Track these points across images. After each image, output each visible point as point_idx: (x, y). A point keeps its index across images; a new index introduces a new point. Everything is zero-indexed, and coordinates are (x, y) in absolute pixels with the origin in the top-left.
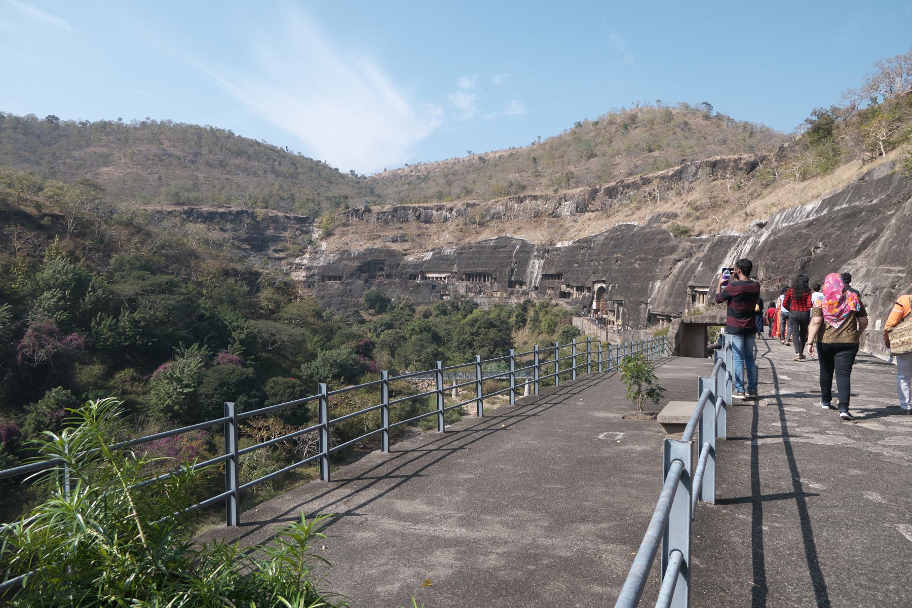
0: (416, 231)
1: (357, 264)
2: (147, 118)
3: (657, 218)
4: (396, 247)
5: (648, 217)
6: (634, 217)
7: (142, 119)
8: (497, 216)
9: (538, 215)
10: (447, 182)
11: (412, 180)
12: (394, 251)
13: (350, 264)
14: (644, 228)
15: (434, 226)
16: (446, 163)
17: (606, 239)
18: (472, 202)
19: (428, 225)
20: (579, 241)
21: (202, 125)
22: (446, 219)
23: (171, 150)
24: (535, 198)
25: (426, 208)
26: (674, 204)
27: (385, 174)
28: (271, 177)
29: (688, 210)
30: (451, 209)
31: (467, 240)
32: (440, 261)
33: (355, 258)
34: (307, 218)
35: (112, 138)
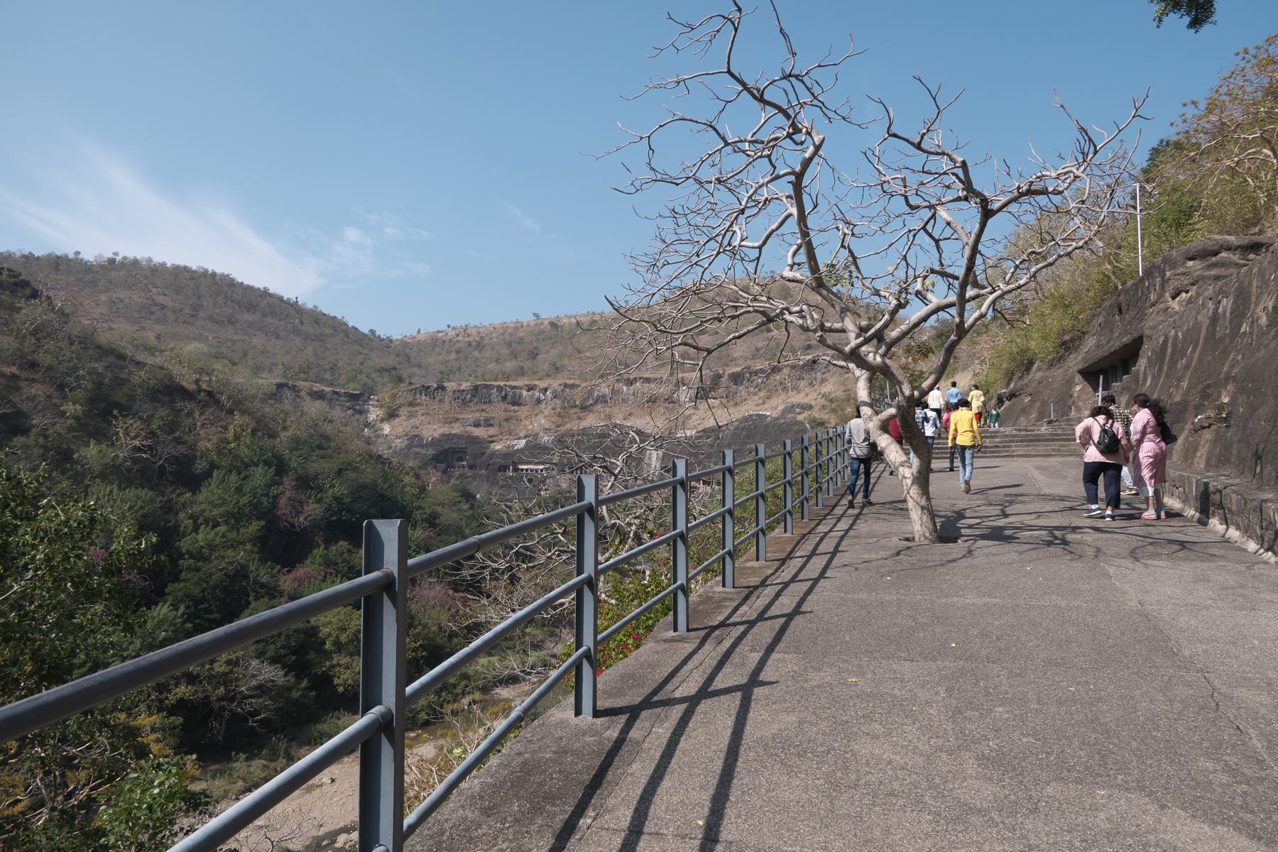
0: (503, 415)
1: (431, 452)
2: (116, 254)
3: (791, 409)
4: (479, 432)
5: (781, 408)
6: (766, 406)
7: (108, 255)
8: (602, 400)
9: (653, 400)
10: (512, 352)
11: (465, 348)
12: (477, 437)
13: (423, 451)
14: (777, 418)
15: (525, 409)
16: (505, 327)
17: (737, 428)
18: (571, 382)
19: (516, 408)
20: (703, 431)
21: (194, 266)
22: (539, 401)
23: (161, 299)
24: (648, 380)
25: (514, 387)
26: (807, 395)
27: (419, 337)
28: (298, 341)
29: (823, 401)
30: (546, 390)
31: (568, 426)
32: (535, 450)
33: (427, 445)
34: (361, 395)
35: (71, 279)
